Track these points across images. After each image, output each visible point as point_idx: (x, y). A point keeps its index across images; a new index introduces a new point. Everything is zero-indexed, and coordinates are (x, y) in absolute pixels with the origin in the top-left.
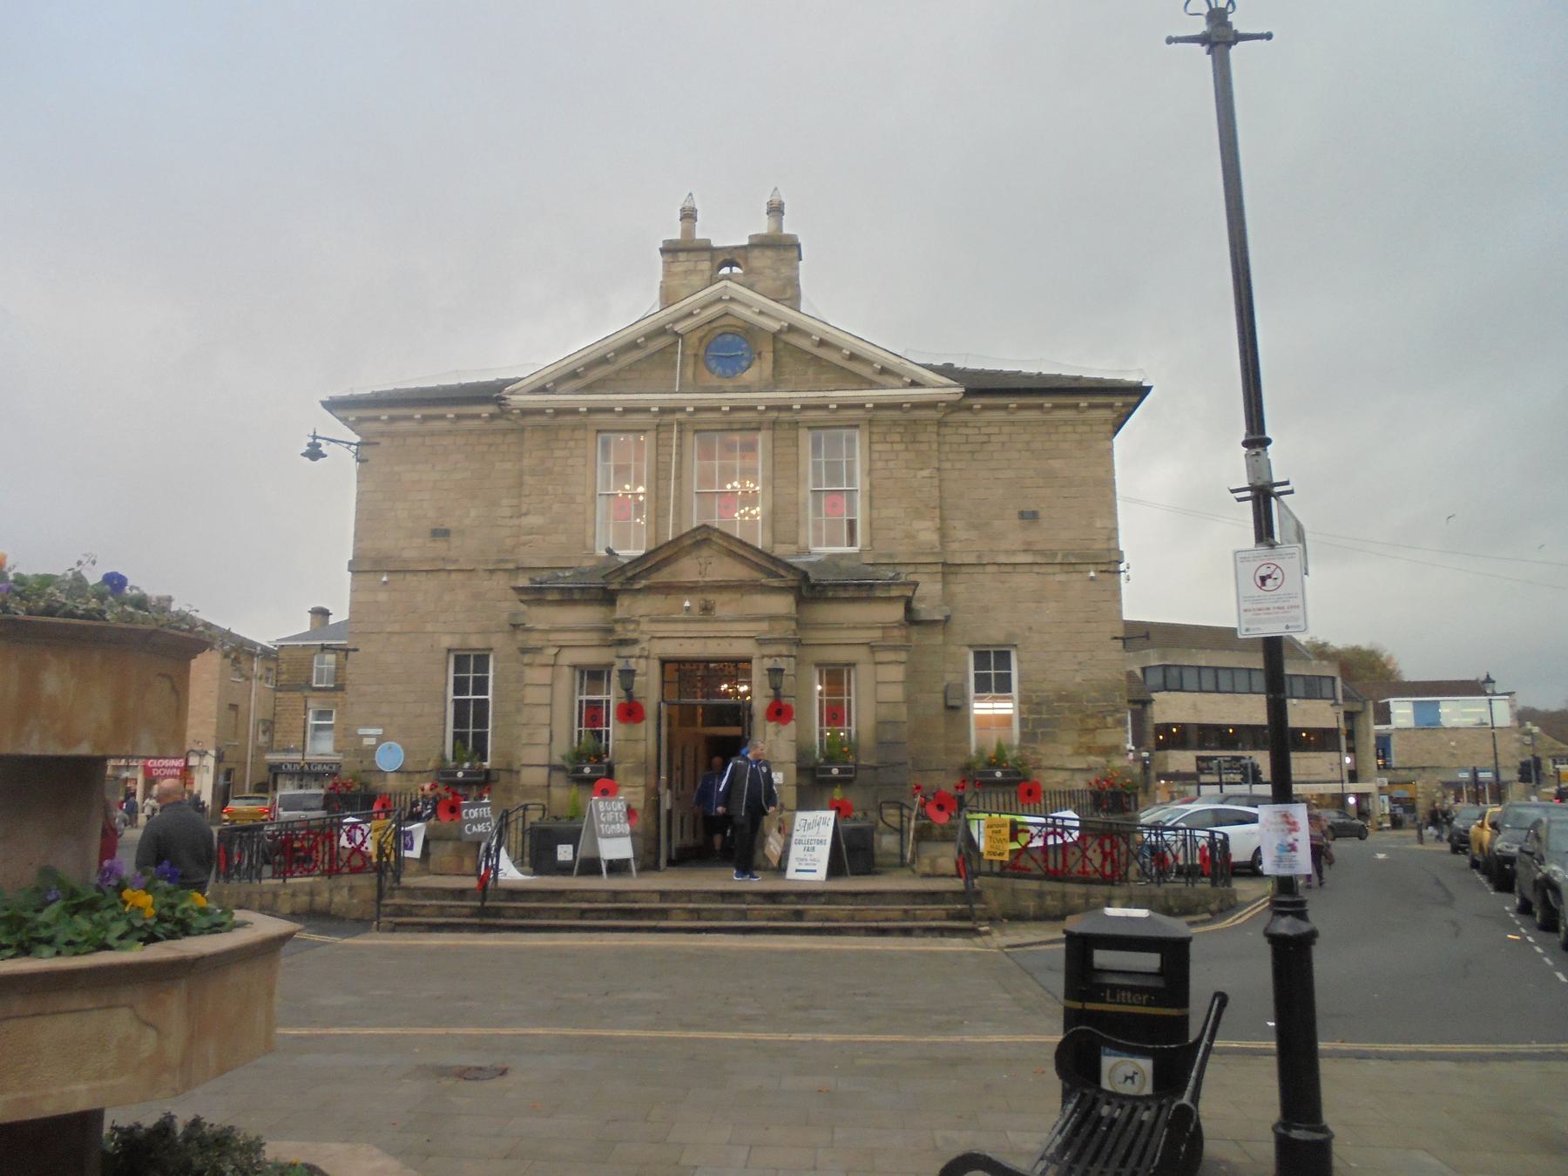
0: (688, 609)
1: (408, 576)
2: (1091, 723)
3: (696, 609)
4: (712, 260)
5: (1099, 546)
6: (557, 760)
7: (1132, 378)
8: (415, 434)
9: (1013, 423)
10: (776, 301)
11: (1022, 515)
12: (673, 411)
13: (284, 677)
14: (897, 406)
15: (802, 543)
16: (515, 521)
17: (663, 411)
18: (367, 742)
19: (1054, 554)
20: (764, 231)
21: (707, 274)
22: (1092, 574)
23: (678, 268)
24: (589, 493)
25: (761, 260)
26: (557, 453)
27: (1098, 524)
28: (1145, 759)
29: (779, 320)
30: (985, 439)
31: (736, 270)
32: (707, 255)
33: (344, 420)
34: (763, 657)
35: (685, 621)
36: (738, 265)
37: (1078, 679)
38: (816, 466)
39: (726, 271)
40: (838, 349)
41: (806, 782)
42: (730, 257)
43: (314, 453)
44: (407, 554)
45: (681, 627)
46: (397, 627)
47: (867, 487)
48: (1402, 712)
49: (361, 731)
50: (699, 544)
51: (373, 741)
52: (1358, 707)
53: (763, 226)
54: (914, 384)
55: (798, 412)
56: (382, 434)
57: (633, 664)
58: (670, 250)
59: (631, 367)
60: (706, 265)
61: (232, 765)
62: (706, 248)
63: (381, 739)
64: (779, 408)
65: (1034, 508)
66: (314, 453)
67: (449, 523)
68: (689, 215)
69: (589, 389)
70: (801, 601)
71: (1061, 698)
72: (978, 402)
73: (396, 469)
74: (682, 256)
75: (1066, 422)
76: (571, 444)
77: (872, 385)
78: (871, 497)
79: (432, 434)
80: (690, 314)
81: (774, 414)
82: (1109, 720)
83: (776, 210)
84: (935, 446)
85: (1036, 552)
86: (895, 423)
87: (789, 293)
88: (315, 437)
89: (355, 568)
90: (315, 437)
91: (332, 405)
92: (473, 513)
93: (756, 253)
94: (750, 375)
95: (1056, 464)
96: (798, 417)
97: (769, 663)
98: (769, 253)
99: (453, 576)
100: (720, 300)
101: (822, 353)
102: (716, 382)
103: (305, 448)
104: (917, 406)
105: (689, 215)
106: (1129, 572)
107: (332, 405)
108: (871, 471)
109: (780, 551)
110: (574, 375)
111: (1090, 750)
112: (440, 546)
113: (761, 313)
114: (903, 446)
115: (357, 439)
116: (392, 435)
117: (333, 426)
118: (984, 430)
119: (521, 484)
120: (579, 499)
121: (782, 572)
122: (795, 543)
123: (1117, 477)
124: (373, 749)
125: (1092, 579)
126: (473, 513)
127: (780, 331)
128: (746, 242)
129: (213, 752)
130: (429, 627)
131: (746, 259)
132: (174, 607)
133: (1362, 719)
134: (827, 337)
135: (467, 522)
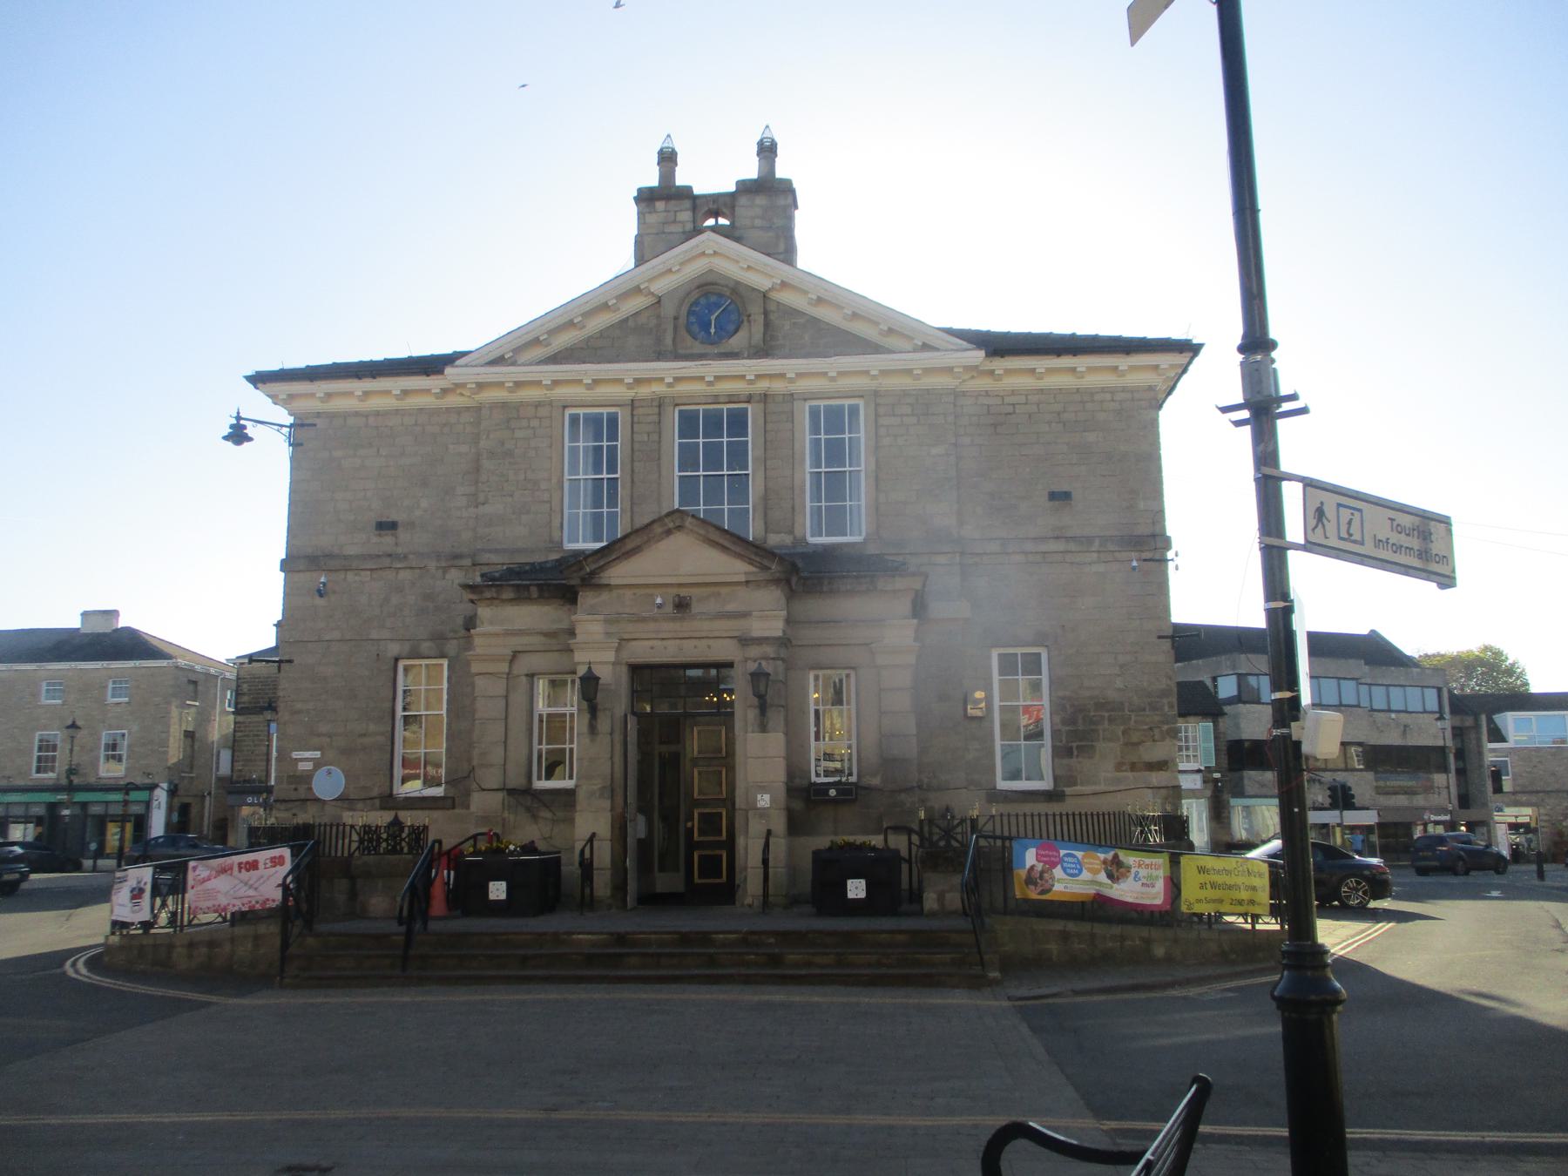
0: (660, 606)
1: (350, 576)
2: (1135, 738)
3: (669, 609)
4: (694, 209)
5: (1143, 530)
6: (511, 784)
7: (1176, 333)
8: (357, 414)
9: (1041, 391)
10: (768, 255)
11: (1053, 496)
12: (649, 381)
13: (245, 699)
14: (909, 372)
15: (798, 533)
16: (472, 510)
17: (638, 381)
18: (302, 766)
19: (1089, 540)
20: (754, 175)
21: (689, 227)
22: (1135, 564)
23: (652, 219)
24: (554, 480)
25: (749, 210)
27: (1142, 505)
28: (1216, 780)
30: (1010, 409)
31: (722, 221)
32: (687, 204)
33: (275, 399)
34: (746, 660)
35: (655, 620)
36: (724, 216)
37: (1119, 683)
38: (816, 443)
39: (711, 222)
40: (838, 307)
41: (798, 805)
42: (717, 204)
43: (238, 435)
44: (351, 550)
45: (652, 626)
46: (336, 635)
47: (873, 466)
48: (1519, 728)
49: (295, 755)
50: (669, 532)
51: (309, 766)
52: (1469, 721)
53: (751, 171)
54: (926, 347)
55: (791, 381)
56: (318, 415)
57: (597, 671)
58: (646, 198)
59: (602, 334)
60: (686, 216)
61: (186, 800)
62: (686, 193)
63: (318, 764)
64: (771, 376)
65: (1065, 488)
66: (238, 435)
67: (394, 517)
68: (667, 159)
69: (554, 359)
70: (791, 595)
71: (1100, 706)
72: (1000, 364)
73: (338, 453)
74: (660, 205)
75: (1103, 390)
76: (535, 423)
77: (876, 349)
78: (877, 479)
79: (377, 414)
82: (1156, 731)
83: (767, 150)
84: (951, 419)
85: (1068, 539)
86: (906, 393)
87: (782, 246)
88: (239, 418)
89: (286, 566)
90: (239, 418)
91: (259, 379)
92: (424, 504)
93: (743, 200)
94: (737, 341)
95: (1091, 437)
96: (793, 388)
97: (752, 667)
98: (761, 200)
99: (404, 575)
100: (703, 254)
101: (823, 313)
102: (698, 348)
103: (227, 431)
104: (928, 371)
105: (667, 159)
106: (1178, 561)
107: (259, 379)
108: (877, 448)
109: (774, 540)
110: (536, 342)
111: (1133, 767)
112: (388, 539)
114: (913, 420)
115: (291, 420)
116: (332, 416)
117: (258, 404)
118: (1007, 400)
119: (478, 470)
120: (543, 486)
121: (766, 562)
122: (791, 532)
123: (1163, 452)
124: (307, 778)
125: (1134, 568)
126: (424, 504)
128: (733, 188)
129: (165, 786)
130: (374, 635)
131: (733, 208)
132: (123, 622)
133: (1473, 736)
135: (418, 513)
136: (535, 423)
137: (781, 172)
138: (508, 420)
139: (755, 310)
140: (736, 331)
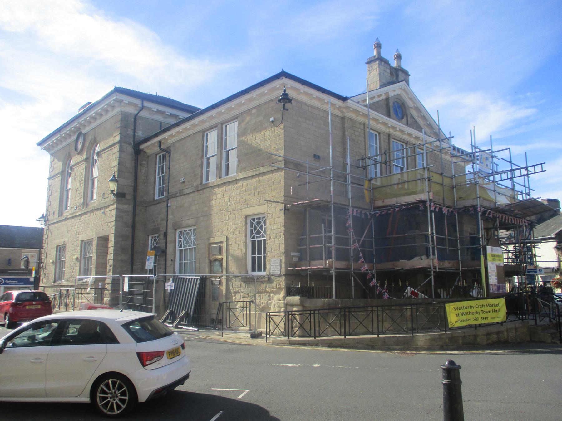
8: (305, 104)
26: (356, 133)
29: (414, 103)
60: (388, 71)
62: (386, 62)
67: (318, 154)
68: (378, 46)
74: (383, 63)
76: (359, 130)
79: (312, 107)
80: (394, 91)
81: (412, 139)
93: (400, 73)
94: (404, 120)
98: (403, 75)
113: (411, 99)
116: (297, 101)
127: (412, 108)
134: (426, 116)
136: (359, 130)
137: (404, 66)
138: (353, 126)
139: (408, 113)
140: (402, 118)
